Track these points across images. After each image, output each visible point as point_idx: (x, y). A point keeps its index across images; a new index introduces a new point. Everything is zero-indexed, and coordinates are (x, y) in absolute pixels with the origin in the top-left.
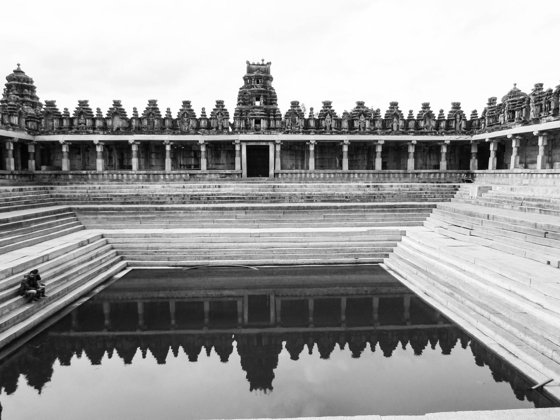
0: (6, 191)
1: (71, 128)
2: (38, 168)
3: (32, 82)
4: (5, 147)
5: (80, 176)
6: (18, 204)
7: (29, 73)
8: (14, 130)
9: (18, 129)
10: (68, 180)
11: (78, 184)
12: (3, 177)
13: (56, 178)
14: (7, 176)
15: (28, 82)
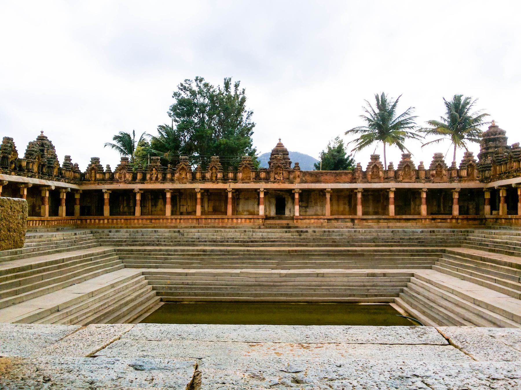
0: (413, 232)
1: (505, 173)
2: (491, 214)
3: (503, 133)
4: (452, 195)
5: (508, 221)
6: (410, 242)
7: (501, 126)
8: (460, 181)
9: (465, 180)
10: (501, 224)
11: (504, 228)
12: (443, 221)
13: (496, 222)
14: (449, 220)
15: (495, 135)
